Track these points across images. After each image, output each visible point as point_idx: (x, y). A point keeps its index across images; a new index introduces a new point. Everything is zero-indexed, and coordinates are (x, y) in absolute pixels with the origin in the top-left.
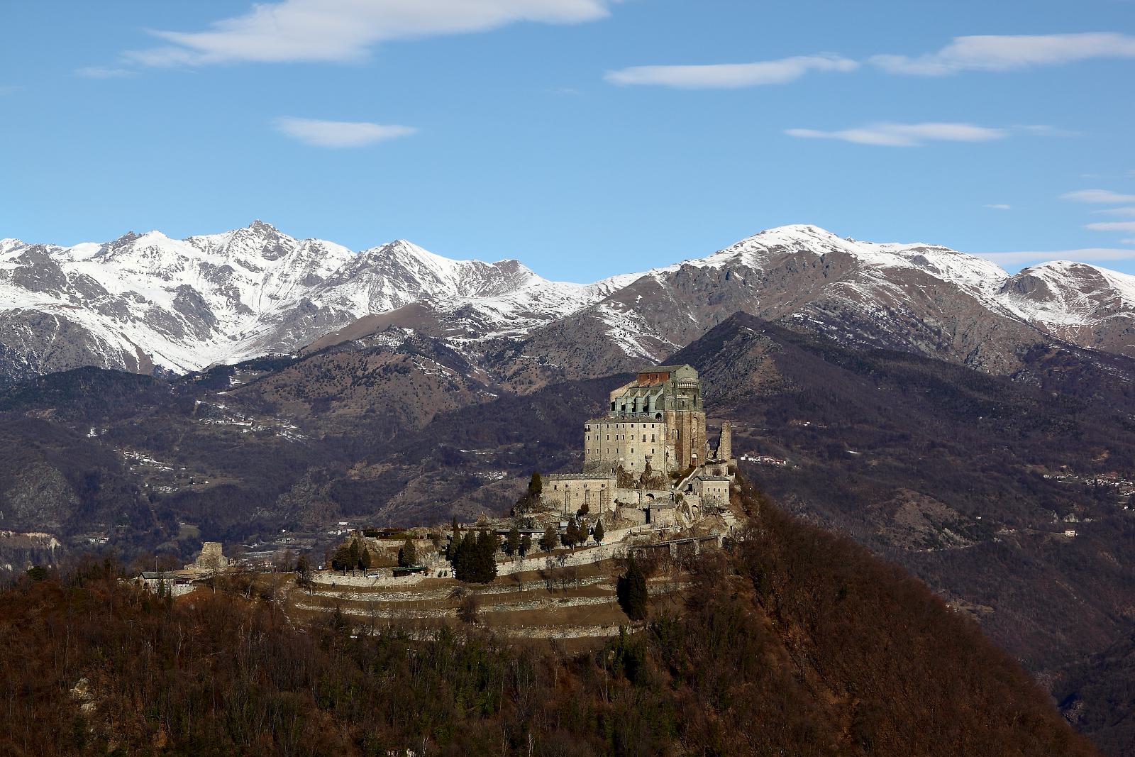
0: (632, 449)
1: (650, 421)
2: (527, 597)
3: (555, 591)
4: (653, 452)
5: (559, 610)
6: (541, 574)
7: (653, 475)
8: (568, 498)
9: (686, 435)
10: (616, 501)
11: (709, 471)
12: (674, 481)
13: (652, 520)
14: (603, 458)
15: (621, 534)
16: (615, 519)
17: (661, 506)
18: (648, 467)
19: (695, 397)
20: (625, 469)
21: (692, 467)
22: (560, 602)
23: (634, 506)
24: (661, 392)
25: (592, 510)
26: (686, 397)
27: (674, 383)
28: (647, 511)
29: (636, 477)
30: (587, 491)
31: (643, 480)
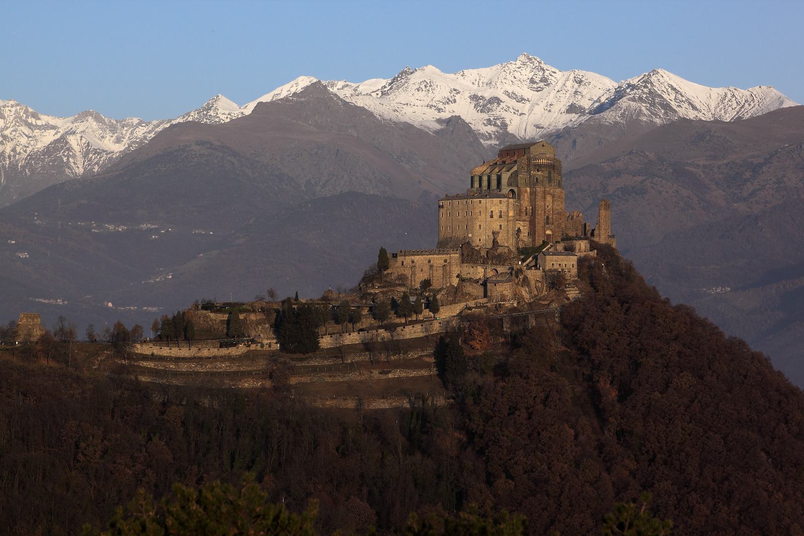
0: (480, 226)
1: (504, 196)
2: (352, 367)
3: (378, 362)
4: (501, 228)
5: (379, 380)
6: (367, 346)
7: (500, 250)
8: (414, 274)
9: (539, 211)
10: (457, 277)
11: (560, 247)
12: (522, 257)
13: (489, 294)
14: (454, 235)
15: (457, 309)
16: (456, 294)
17: (498, 281)
18: (495, 242)
19: (550, 173)
20: (474, 244)
21: (545, 244)
22: (380, 373)
23: (477, 281)
24: (515, 168)
25: (436, 285)
26: (540, 173)
27: (529, 159)
28: (484, 284)
29: (483, 253)
30: (431, 266)
31: (489, 255)
